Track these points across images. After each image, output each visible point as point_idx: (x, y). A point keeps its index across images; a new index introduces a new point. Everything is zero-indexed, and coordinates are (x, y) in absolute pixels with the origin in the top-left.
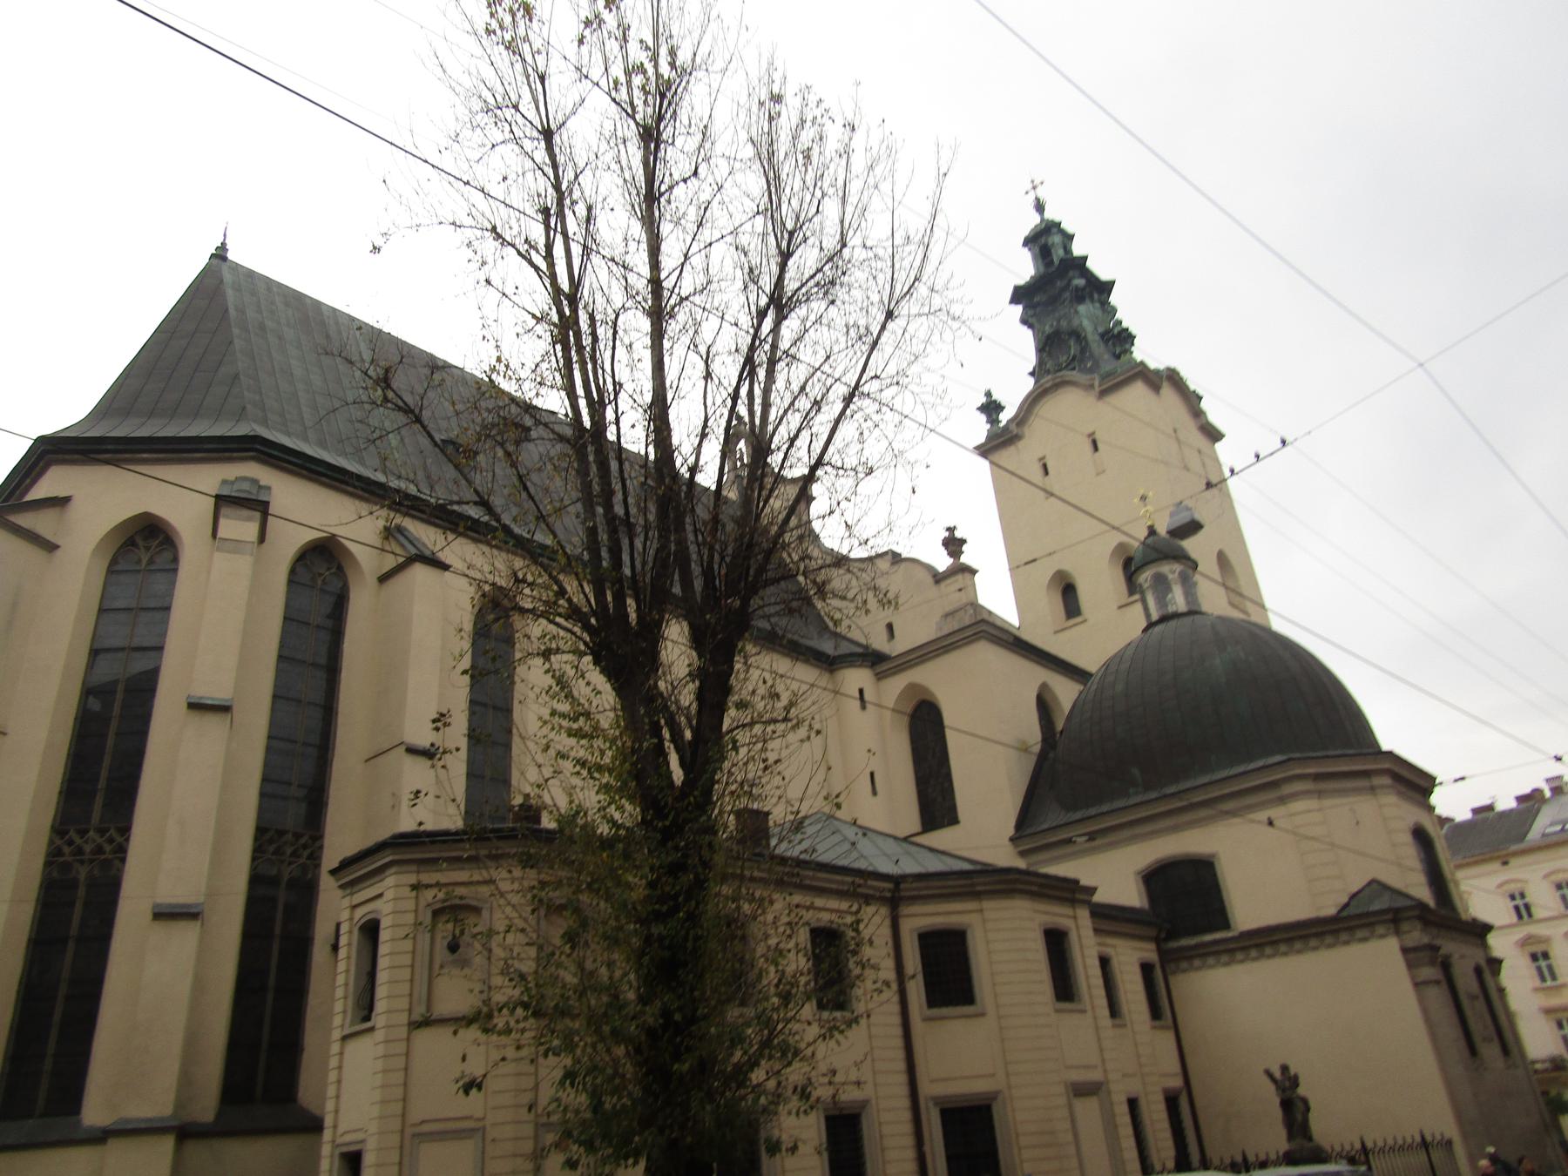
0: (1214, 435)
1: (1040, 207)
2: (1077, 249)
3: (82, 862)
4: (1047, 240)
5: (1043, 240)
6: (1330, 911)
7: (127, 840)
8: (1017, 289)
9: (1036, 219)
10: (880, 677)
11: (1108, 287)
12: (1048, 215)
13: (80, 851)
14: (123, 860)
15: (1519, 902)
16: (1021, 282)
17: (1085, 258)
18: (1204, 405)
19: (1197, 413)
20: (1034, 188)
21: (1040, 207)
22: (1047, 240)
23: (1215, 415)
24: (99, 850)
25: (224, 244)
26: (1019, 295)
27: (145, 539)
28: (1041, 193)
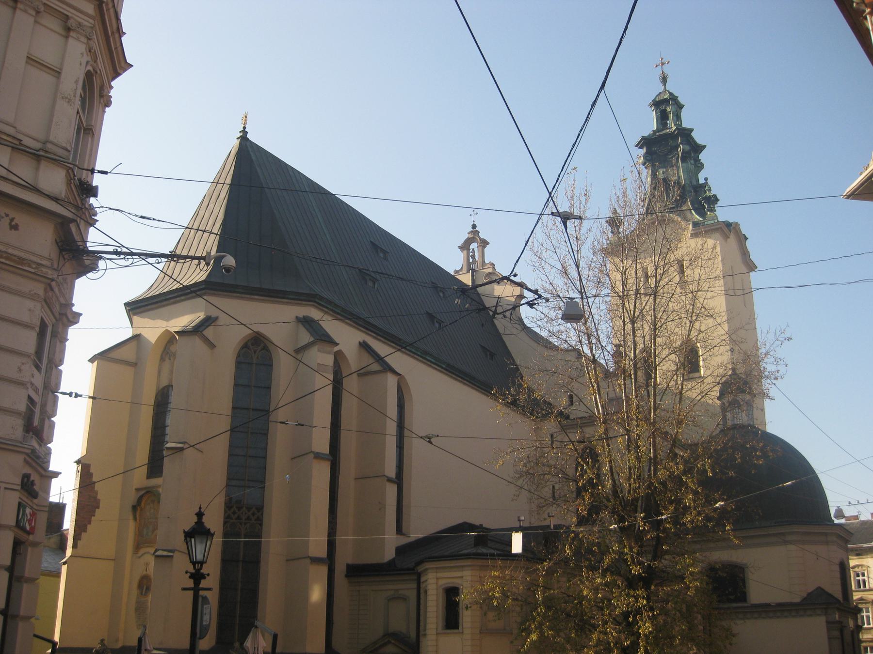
0: (751, 267)
1: (664, 79)
2: (686, 122)
3: (241, 524)
4: (666, 106)
5: (663, 107)
6: (797, 600)
7: (262, 514)
8: (643, 138)
9: (662, 88)
10: (564, 429)
11: (699, 148)
12: (670, 87)
13: (238, 518)
14: (261, 525)
15: (861, 578)
16: (646, 134)
17: (692, 130)
18: (748, 243)
19: (745, 253)
20: (663, 64)
21: (664, 79)
22: (666, 106)
23: (755, 256)
24: (248, 518)
25: (244, 132)
26: (645, 142)
27: (252, 344)
28: (667, 69)
